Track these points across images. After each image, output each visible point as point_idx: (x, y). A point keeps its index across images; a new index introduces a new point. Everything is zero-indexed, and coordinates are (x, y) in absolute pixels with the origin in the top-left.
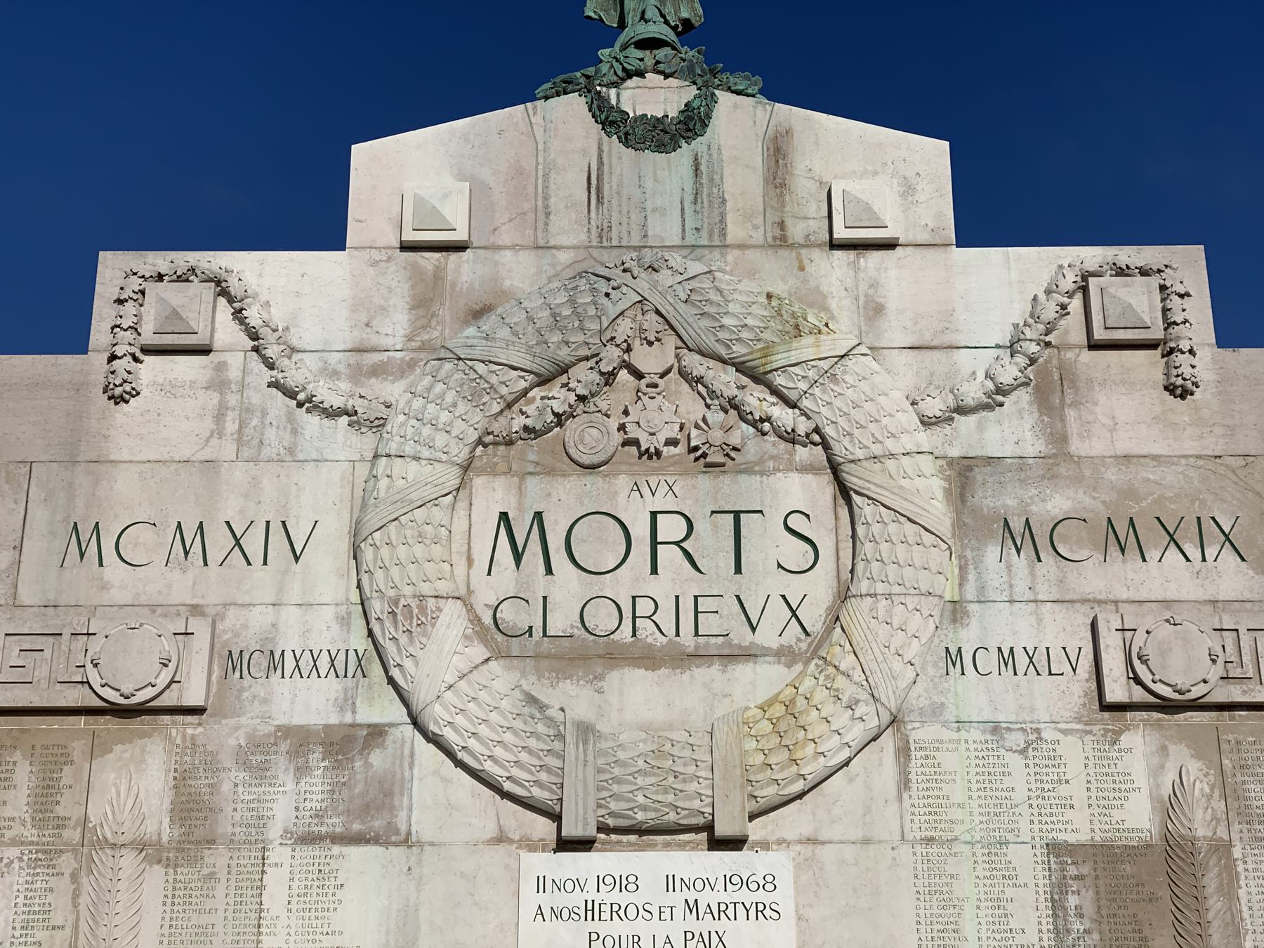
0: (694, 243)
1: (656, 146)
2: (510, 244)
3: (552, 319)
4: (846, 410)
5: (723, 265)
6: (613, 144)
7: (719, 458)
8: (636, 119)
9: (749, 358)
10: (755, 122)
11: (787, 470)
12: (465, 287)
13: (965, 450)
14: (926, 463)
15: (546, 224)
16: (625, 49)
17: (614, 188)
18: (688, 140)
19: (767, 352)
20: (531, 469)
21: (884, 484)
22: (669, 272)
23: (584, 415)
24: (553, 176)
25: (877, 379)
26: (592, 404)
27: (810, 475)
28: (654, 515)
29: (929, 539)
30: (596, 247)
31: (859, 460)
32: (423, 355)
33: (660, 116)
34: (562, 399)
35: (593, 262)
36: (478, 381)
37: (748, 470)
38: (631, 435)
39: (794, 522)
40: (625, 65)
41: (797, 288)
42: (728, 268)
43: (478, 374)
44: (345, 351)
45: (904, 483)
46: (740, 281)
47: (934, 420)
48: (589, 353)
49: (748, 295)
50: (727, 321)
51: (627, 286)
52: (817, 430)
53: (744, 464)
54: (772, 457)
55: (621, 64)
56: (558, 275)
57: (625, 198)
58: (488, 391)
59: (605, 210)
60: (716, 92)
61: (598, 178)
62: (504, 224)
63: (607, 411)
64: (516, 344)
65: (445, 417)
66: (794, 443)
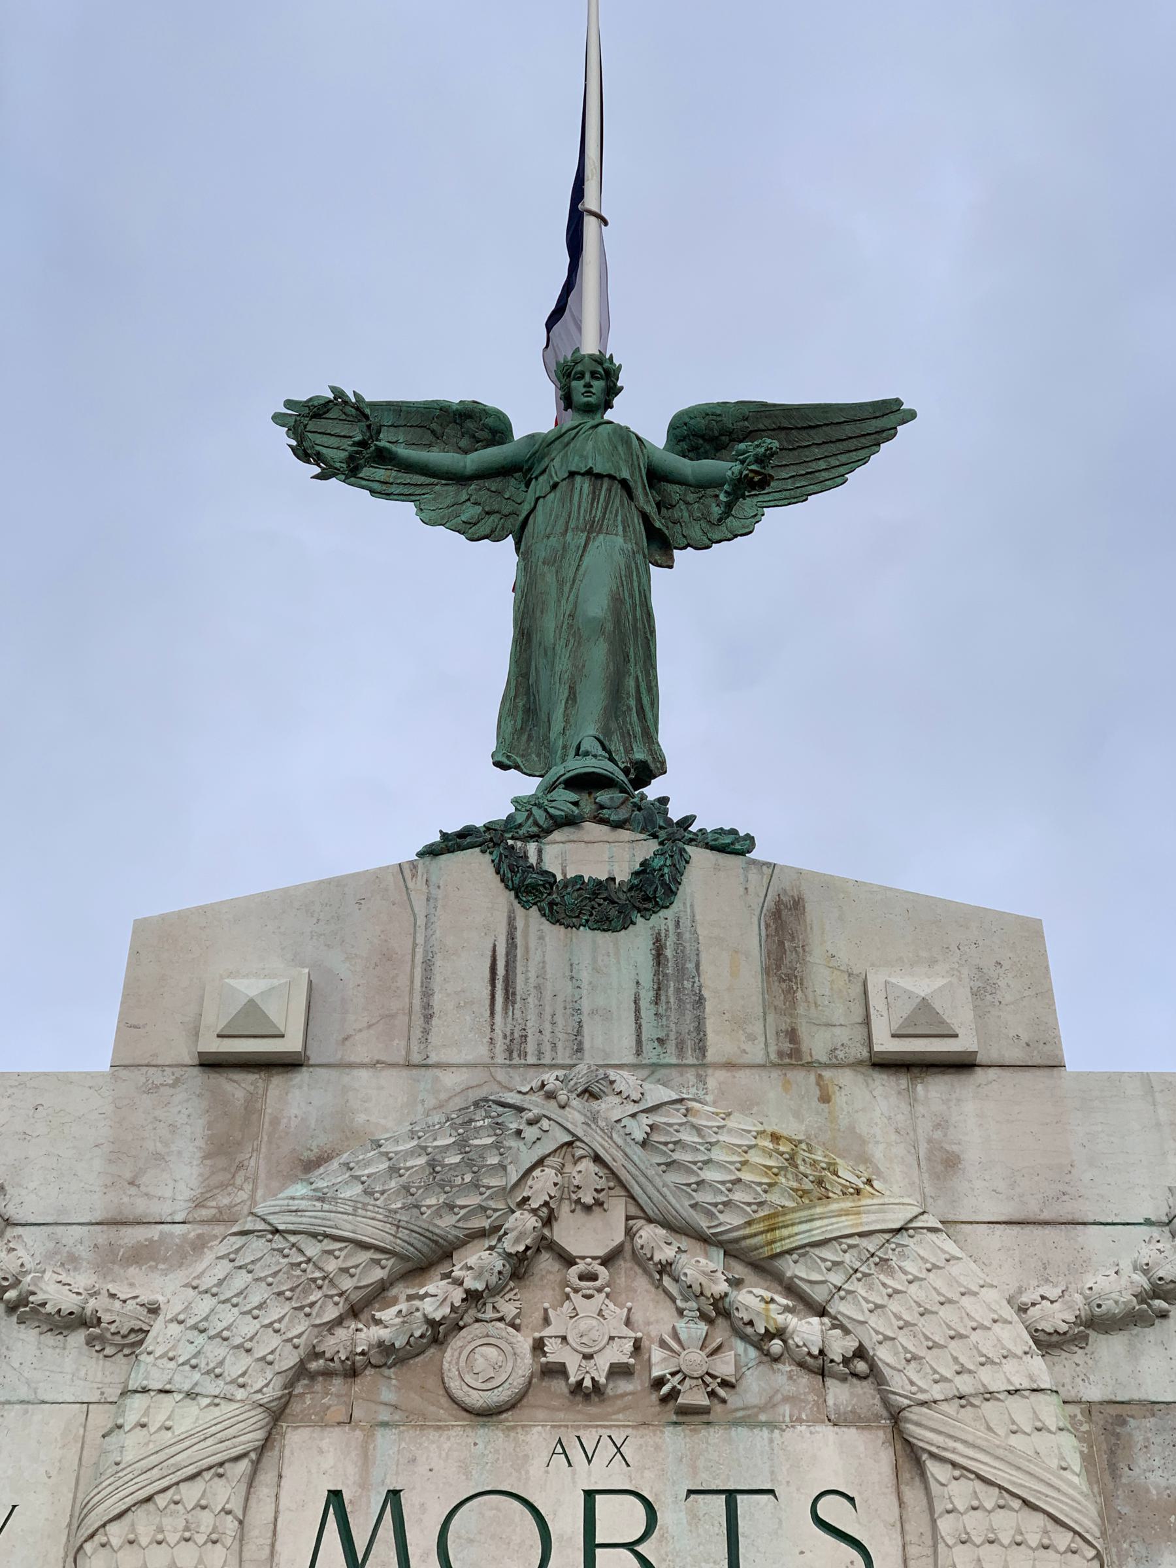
0: (654, 1060)
1: (596, 922)
2: (366, 1060)
3: (428, 1170)
4: (907, 1317)
5: (701, 1093)
6: (532, 921)
7: (700, 1398)
8: (566, 883)
9: (747, 1231)
10: (746, 889)
11: (816, 1421)
12: (293, 1124)
13: (1110, 1389)
14: (1049, 1411)
15: (426, 1032)
16: (550, 792)
17: (531, 980)
18: (646, 913)
19: (775, 1221)
20: (384, 1415)
21: (979, 1442)
22: (617, 1100)
23: (477, 1325)
24: (438, 962)
25: (955, 1269)
26: (489, 1307)
27: (853, 1430)
28: (590, 1496)
29: (1063, 1539)
30: (503, 1066)
31: (935, 1402)
32: (219, 1230)
33: (603, 878)
34: (440, 1298)
35: (496, 1088)
36: (304, 1266)
37: (749, 1421)
38: (551, 1358)
39: (830, 1510)
40: (551, 811)
41: (820, 1129)
42: (709, 1098)
43: (305, 1255)
44: (92, 1224)
45: (1014, 1440)
46: (729, 1114)
47: (1055, 1338)
48: (486, 1224)
49: (742, 1135)
50: (709, 1175)
51: (550, 1119)
52: (860, 1353)
53: (743, 1409)
54: (786, 1399)
55: (546, 810)
56: (441, 1106)
57: (548, 995)
58: (320, 1282)
59: (518, 1013)
60: (687, 848)
61: (507, 966)
62: (360, 1031)
63: (515, 1317)
64: (370, 1208)
65: (248, 1327)
66: (823, 1375)
